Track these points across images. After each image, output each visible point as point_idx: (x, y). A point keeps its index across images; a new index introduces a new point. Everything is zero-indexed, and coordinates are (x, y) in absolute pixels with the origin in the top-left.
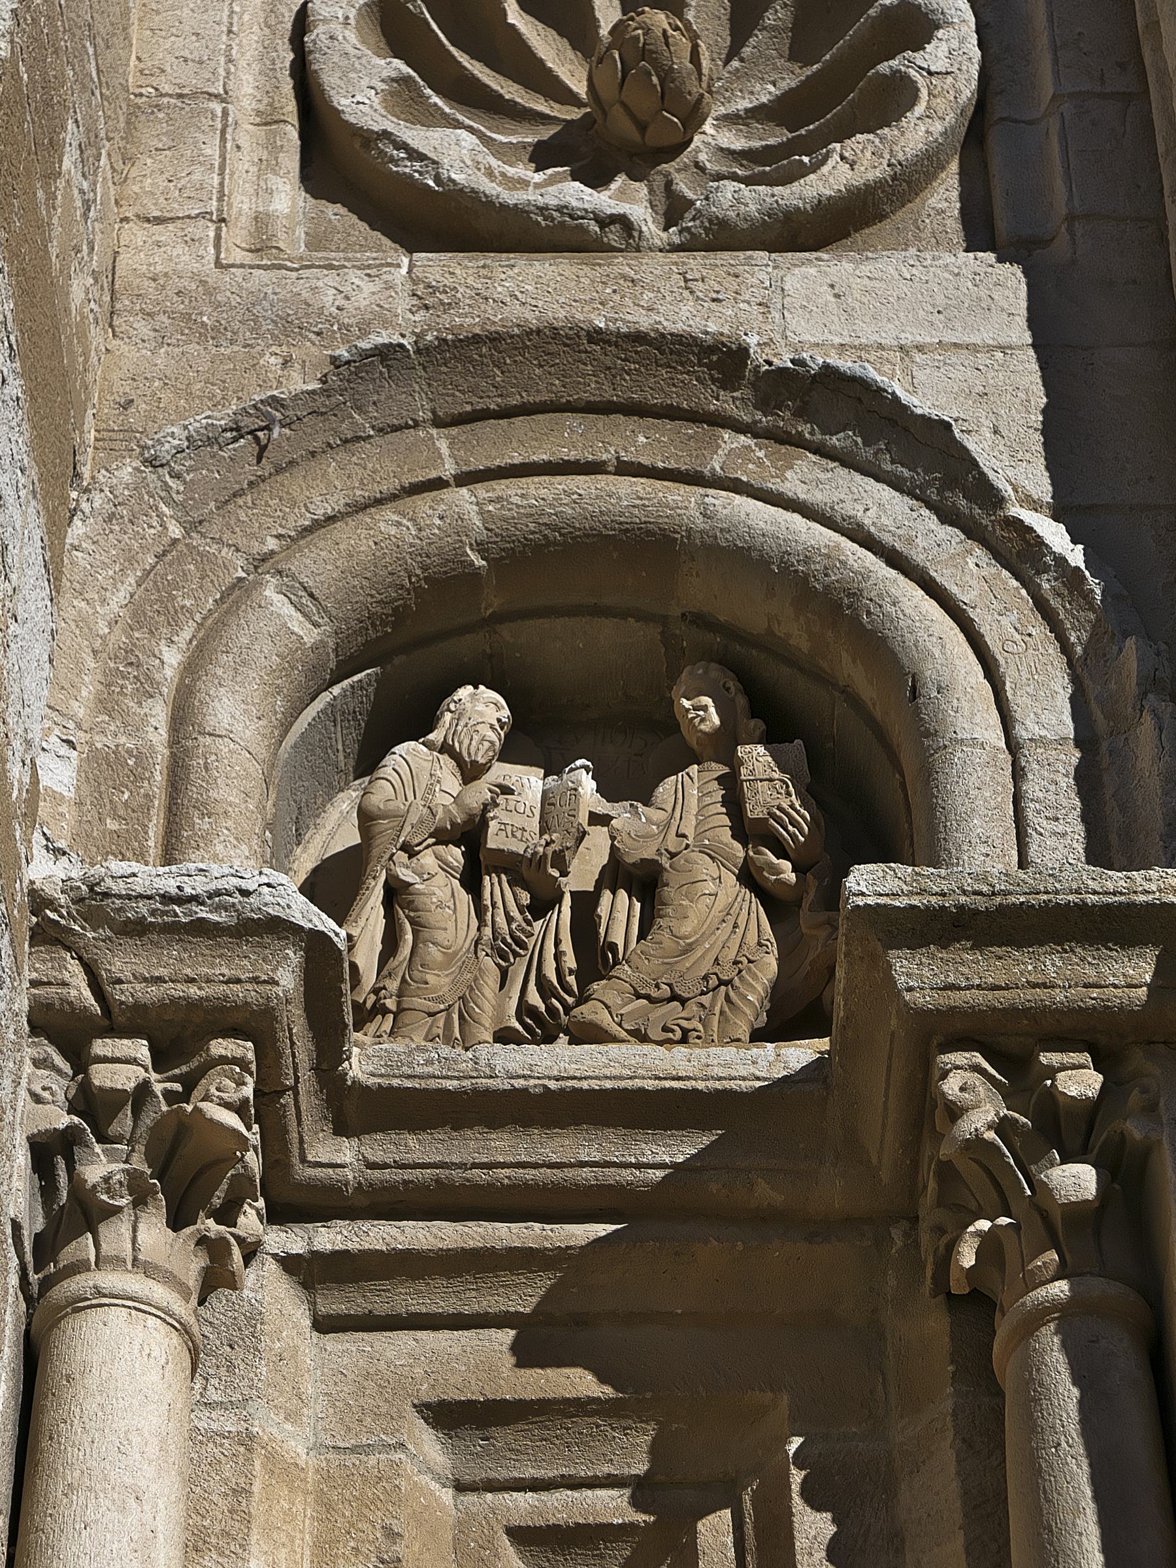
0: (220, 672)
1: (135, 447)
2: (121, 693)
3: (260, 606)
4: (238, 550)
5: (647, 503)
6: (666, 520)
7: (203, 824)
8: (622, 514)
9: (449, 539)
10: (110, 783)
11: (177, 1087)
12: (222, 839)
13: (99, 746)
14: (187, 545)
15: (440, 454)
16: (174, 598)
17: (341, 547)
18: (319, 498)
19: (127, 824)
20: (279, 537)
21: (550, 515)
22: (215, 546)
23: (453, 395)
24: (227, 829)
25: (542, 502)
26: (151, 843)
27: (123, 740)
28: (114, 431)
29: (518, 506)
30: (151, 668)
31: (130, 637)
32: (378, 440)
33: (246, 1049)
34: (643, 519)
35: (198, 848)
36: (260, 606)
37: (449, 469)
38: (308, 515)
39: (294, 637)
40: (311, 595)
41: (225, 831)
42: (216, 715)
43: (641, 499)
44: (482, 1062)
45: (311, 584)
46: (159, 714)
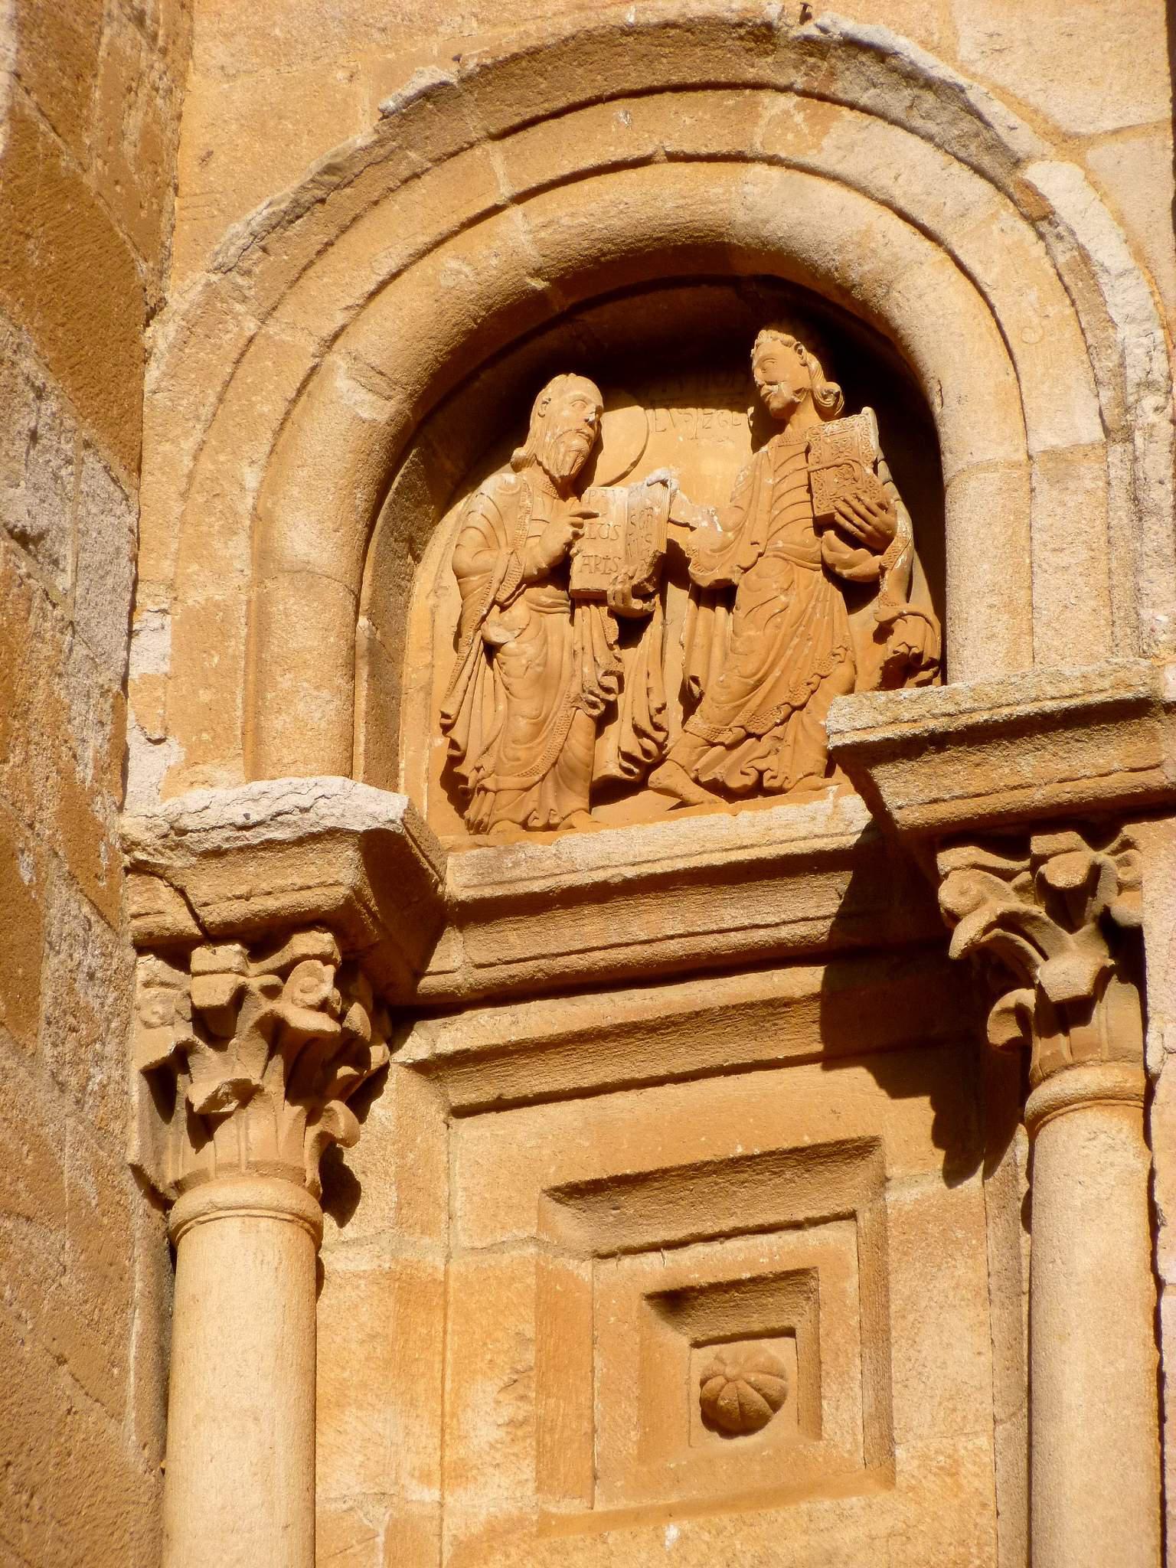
0: (295, 491)
1: (216, 213)
3: (332, 402)
4: (311, 334)
5: (690, 201)
6: (710, 216)
7: (285, 682)
8: (667, 217)
9: (507, 276)
11: (273, 980)
12: (302, 694)
14: (264, 335)
15: (495, 174)
17: (405, 312)
18: (383, 254)
20: (347, 308)
21: (600, 230)
22: (290, 332)
23: (501, 111)
24: (306, 680)
25: (592, 219)
28: (196, 195)
29: (569, 227)
30: (235, 498)
31: (215, 462)
32: (437, 170)
33: (321, 941)
34: (688, 219)
35: (279, 711)
36: (332, 402)
37: (506, 191)
39: (366, 425)
41: (305, 685)
45: (378, 362)
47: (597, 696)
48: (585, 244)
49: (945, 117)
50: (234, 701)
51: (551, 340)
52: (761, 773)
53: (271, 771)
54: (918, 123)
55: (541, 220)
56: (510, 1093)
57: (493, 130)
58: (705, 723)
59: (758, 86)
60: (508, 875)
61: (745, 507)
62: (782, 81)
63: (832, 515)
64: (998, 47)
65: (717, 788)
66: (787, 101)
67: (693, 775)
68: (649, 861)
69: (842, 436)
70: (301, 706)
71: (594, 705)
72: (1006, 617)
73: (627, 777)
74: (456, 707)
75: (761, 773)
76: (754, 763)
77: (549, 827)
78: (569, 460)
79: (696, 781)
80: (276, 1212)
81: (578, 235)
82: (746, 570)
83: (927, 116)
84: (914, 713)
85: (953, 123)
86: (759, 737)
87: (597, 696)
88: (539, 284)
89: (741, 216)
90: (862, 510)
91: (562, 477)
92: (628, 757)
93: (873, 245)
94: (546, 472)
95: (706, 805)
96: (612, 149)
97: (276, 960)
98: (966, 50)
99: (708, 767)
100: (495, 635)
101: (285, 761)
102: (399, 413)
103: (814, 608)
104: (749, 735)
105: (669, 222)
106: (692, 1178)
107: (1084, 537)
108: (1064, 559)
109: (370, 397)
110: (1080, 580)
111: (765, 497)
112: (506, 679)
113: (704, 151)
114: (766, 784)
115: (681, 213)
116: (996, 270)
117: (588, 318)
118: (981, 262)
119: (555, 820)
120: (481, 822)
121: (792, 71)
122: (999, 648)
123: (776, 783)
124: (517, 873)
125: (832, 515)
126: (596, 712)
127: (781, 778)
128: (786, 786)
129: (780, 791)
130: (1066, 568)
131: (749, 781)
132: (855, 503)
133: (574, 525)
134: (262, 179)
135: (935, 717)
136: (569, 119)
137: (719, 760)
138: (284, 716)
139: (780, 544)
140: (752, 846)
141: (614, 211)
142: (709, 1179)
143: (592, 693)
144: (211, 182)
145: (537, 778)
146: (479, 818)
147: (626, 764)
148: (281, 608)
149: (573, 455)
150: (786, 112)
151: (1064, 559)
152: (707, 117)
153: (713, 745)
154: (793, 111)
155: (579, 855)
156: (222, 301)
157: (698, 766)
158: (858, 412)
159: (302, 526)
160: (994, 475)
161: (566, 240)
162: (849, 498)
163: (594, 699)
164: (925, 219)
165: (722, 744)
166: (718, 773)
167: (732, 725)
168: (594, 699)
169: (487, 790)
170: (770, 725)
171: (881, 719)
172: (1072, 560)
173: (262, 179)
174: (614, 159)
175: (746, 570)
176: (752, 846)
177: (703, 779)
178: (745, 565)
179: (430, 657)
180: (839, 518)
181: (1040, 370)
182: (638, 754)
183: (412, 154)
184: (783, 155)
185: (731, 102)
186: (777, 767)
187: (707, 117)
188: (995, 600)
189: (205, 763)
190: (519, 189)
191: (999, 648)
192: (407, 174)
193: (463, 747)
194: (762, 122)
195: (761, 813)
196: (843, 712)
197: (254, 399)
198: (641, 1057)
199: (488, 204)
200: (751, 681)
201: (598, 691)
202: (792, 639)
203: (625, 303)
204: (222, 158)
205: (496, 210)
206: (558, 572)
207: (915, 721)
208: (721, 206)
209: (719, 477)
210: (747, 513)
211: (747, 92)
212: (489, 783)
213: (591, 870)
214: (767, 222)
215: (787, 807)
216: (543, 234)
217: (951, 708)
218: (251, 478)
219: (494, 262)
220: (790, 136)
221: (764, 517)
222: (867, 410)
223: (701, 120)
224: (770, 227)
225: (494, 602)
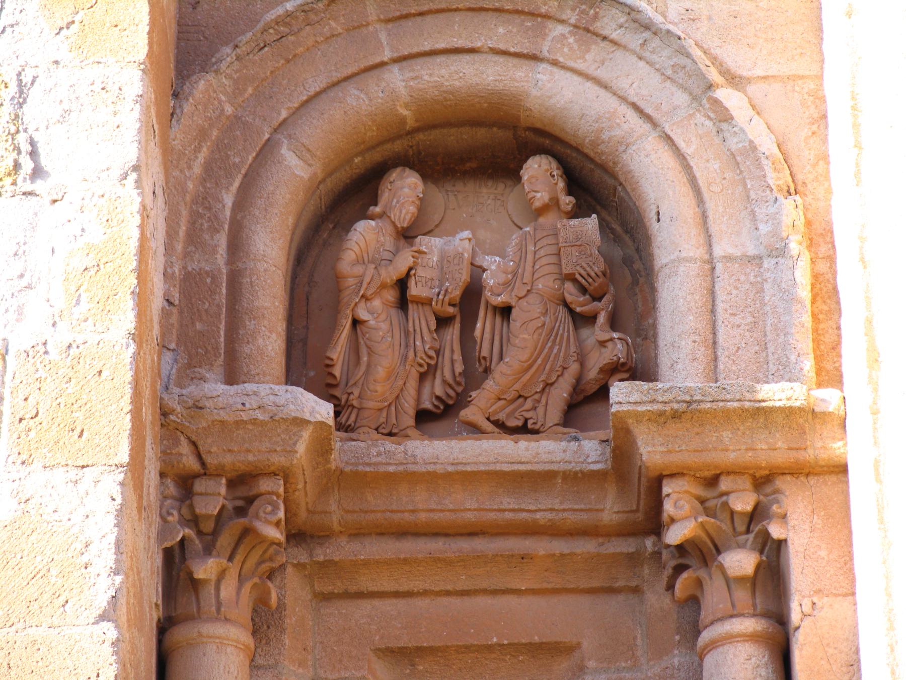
1: (202, 38)
2: (201, 230)
5: (503, 78)
8: (489, 85)
10: (197, 296)
13: (190, 269)
16: (228, 157)
18: (311, 80)
19: (208, 326)
21: (447, 86)
22: (251, 117)
25: (442, 79)
26: (222, 339)
27: (203, 264)
28: (188, 25)
29: (428, 82)
31: (204, 187)
35: (248, 343)
38: (305, 92)
40: (308, 150)
41: (263, 328)
42: (255, 245)
43: (500, 75)
44: (409, 454)
46: (222, 240)
47: (424, 360)
48: (436, 93)
49: (666, 52)
50: (219, 332)
51: (398, 146)
52: (526, 420)
53: (243, 378)
54: (647, 54)
55: (411, 74)
56: (353, 588)
57: (382, 17)
58: (496, 385)
59: (547, 17)
60: (374, 460)
61: (517, 261)
62: (564, 17)
63: (574, 274)
64: (692, 17)
65: (501, 426)
66: (560, 29)
67: (487, 416)
68: (462, 463)
69: (580, 229)
70: (260, 341)
71: (421, 365)
72: (703, 349)
73: (435, 410)
74: (337, 355)
75: (526, 420)
76: (523, 413)
77: (390, 434)
78: (408, 217)
79: (488, 419)
80: (753, 637)
81: (433, 87)
82: (520, 298)
83: (653, 52)
84: (666, 398)
85: (670, 58)
86: (526, 398)
87: (424, 360)
88: (405, 112)
89: (534, 92)
90: (593, 274)
91: (402, 227)
92: (438, 398)
93: (618, 121)
94: (393, 223)
95: (496, 434)
96: (455, 40)
97: (242, 491)
98: (672, 14)
99: (496, 412)
100: (363, 315)
101: (252, 372)
102: (315, 174)
103: (559, 326)
104: (520, 396)
105: (489, 88)
106: (462, 653)
107: (750, 309)
108: (737, 320)
109: (301, 163)
110: (747, 334)
111: (530, 257)
112: (368, 342)
113: (512, 50)
114: (530, 426)
115: (497, 84)
116: (694, 147)
117: (421, 136)
118: (684, 141)
119: (395, 431)
120: (350, 426)
121: (569, 12)
122: (700, 367)
123: (537, 427)
124: (379, 459)
125: (574, 274)
126: (422, 370)
127: (539, 424)
128: (541, 429)
129: (536, 432)
130: (739, 326)
131: (520, 423)
132: (588, 269)
133: (413, 257)
134: (232, 23)
135: (678, 402)
136: (429, 19)
137: (503, 409)
138: (251, 346)
139: (540, 286)
140: (527, 463)
141: (456, 77)
142: (472, 655)
143: (422, 358)
144: (198, 19)
145: (386, 404)
146: (349, 423)
147: (436, 403)
148: (248, 280)
149: (410, 215)
150: (563, 35)
151: (737, 320)
152: (515, 30)
153: (500, 399)
154: (567, 35)
155: (418, 452)
156: (215, 92)
157: (491, 410)
158: (590, 216)
159: (261, 233)
160: (695, 265)
161: (425, 89)
162: (585, 266)
163: (422, 362)
164: (649, 110)
165: (505, 399)
166: (501, 416)
167: (511, 389)
168: (422, 362)
169: (353, 407)
170: (533, 392)
171: (645, 398)
172: (742, 322)
173: (232, 23)
174: (456, 46)
175: (520, 298)
176: (527, 463)
177: (492, 419)
178: (520, 296)
179: (305, 322)
180: (577, 276)
181: (721, 209)
182: (444, 398)
183: (332, 23)
184: (561, 59)
185: (529, 24)
186: (535, 418)
187: (515, 30)
188: (697, 338)
189: (200, 367)
190: (396, 55)
191: (700, 367)
192: (328, 35)
193: (338, 378)
194: (550, 38)
195: (533, 444)
196: (622, 391)
197: (229, 153)
198: (437, 578)
199: (378, 60)
200: (526, 365)
201: (425, 357)
202: (546, 344)
203: (445, 131)
204: (206, 6)
205: (383, 64)
206: (402, 284)
207: (666, 403)
208: (522, 83)
209: (488, 241)
210: (519, 266)
211: (539, 19)
212: (355, 403)
213: (426, 464)
214: (550, 97)
215: (549, 442)
216: (412, 83)
217: (688, 398)
218: (228, 200)
219: (381, 95)
220: (566, 50)
221: (529, 268)
222: (594, 216)
223: (511, 32)
224: (553, 101)
225: (363, 296)
